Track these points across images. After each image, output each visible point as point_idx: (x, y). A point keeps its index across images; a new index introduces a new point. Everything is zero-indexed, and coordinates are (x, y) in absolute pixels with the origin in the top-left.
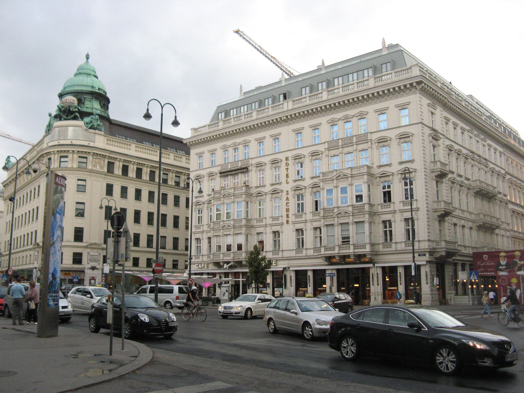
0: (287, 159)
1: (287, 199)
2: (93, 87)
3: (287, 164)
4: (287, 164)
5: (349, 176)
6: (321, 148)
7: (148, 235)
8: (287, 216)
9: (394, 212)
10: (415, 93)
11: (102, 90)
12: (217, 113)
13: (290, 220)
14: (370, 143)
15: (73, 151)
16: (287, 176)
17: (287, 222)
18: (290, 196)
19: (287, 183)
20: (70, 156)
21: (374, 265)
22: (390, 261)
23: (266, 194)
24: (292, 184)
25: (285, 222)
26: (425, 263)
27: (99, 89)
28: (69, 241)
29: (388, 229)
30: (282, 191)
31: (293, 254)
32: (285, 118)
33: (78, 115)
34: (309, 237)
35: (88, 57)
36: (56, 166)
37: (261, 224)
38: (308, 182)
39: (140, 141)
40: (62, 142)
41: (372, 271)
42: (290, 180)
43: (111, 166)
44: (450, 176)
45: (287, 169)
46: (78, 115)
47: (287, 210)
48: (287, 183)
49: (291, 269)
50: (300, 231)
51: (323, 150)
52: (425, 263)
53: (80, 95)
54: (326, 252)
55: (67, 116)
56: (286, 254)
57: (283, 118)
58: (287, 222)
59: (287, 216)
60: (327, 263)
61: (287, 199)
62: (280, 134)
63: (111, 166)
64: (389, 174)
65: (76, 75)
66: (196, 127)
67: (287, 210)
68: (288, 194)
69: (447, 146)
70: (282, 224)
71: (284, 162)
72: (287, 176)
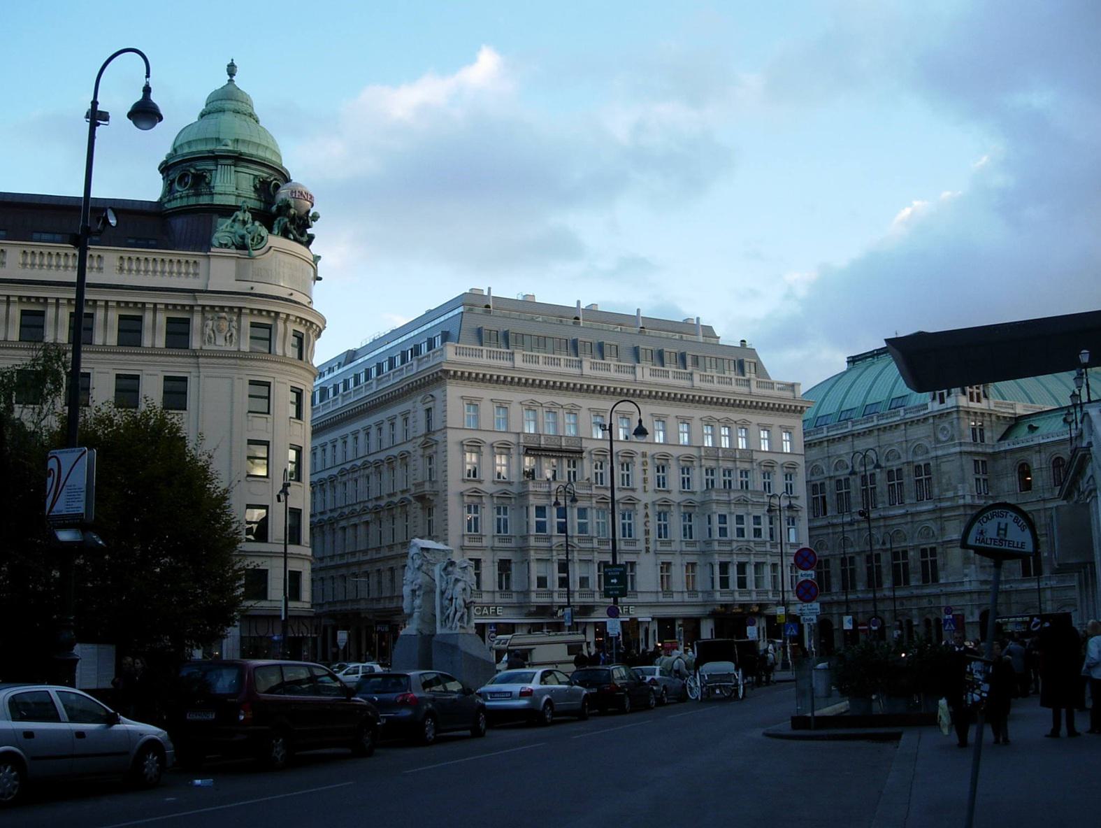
1: (647, 515)
8: (647, 541)
13: (651, 550)
17: (647, 550)
19: (645, 491)
32: (648, 393)
34: (678, 575)
35: (231, 70)
45: (645, 470)
47: (647, 532)
48: (645, 491)
50: (666, 566)
56: (641, 598)
57: (644, 392)
58: (647, 550)
59: (647, 541)
61: (647, 515)
67: (647, 532)
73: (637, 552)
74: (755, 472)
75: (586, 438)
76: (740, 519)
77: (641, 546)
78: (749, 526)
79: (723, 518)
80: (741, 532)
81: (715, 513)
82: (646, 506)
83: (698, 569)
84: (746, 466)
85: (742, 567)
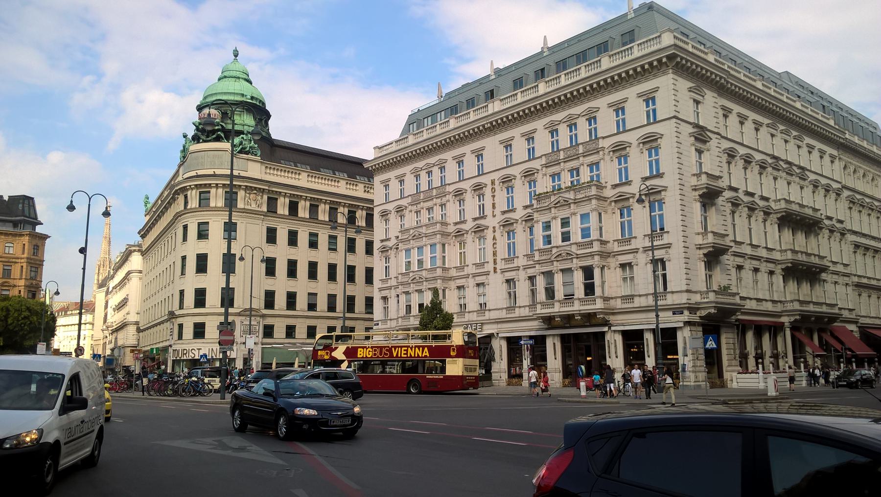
0: (493, 183)
1: (494, 238)
2: (243, 95)
3: (493, 190)
4: (493, 190)
5: (571, 201)
7: (309, 294)
8: (495, 262)
9: (635, 251)
10: (665, 73)
11: (257, 99)
12: (409, 123)
13: (498, 267)
14: (601, 153)
15: (217, 184)
17: (495, 271)
18: (498, 234)
20: (213, 191)
21: (610, 328)
22: (633, 322)
23: (467, 232)
24: (500, 217)
25: (492, 270)
26: (681, 325)
27: (252, 98)
28: (214, 307)
30: (487, 228)
31: (503, 314)
33: (222, 135)
36: (193, 206)
38: (519, 214)
39: (316, 168)
40: (200, 172)
41: (608, 337)
42: (497, 212)
43: (272, 203)
44: (728, 194)
45: (494, 196)
46: (222, 135)
47: (495, 254)
48: (494, 216)
49: (500, 335)
51: (539, 168)
52: (681, 325)
53: (227, 108)
54: (544, 311)
55: (208, 137)
58: (495, 271)
59: (495, 262)
60: (546, 326)
61: (494, 238)
62: (483, 149)
63: (272, 203)
64: (628, 196)
65: (219, 80)
66: (380, 145)
67: (495, 254)
68: (494, 232)
69: (725, 150)
71: (489, 187)
72: (494, 205)
73: (487, 274)
76: (565, 223)
77: (489, 267)
78: (576, 227)
80: (566, 237)
81: (537, 222)
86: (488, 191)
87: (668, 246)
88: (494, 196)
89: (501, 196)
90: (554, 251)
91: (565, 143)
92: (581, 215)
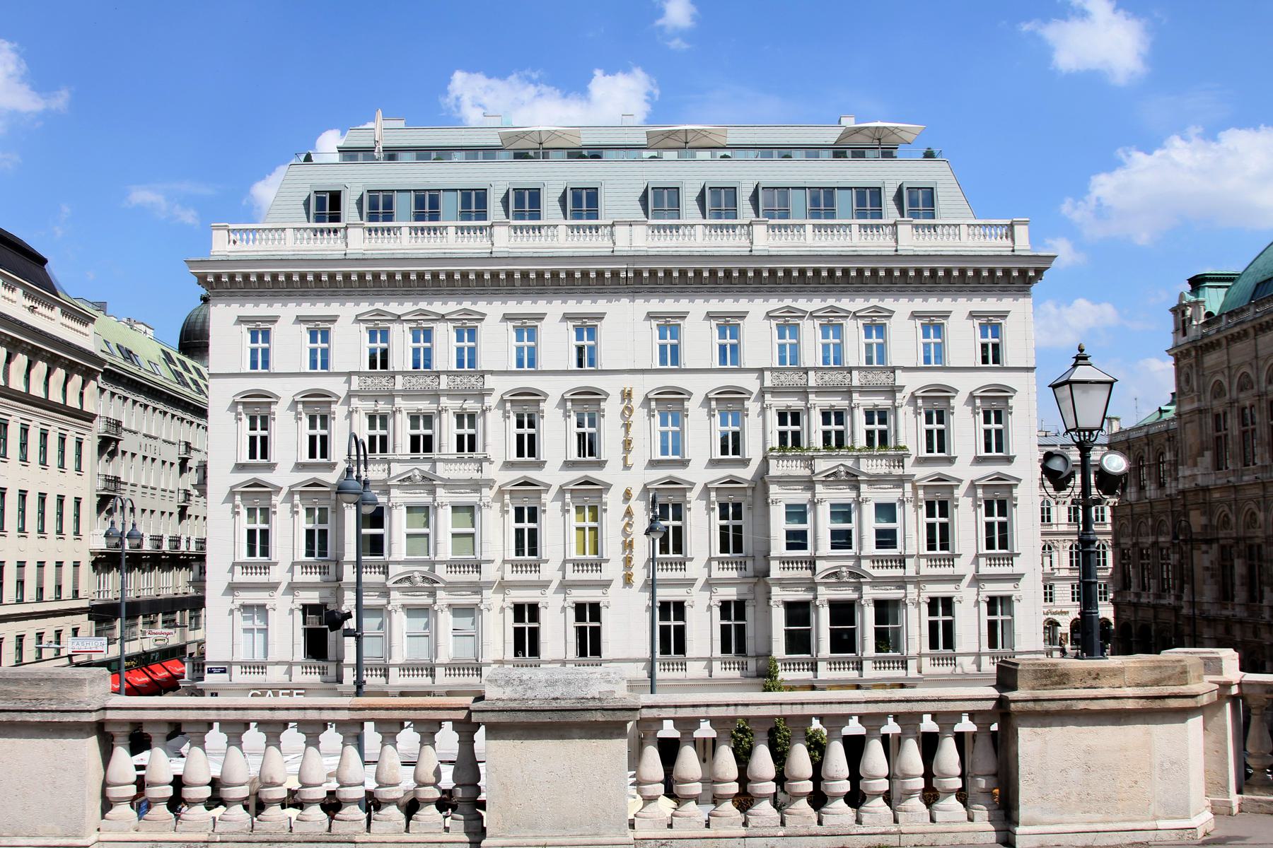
0: (627, 395)
1: (629, 513)
6: (750, 383)
8: (628, 562)
16: (627, 445)
17: (628, 580)
19: (626, 467)
29: (940, 618)
30: (608, 487)
32: (631, 275)
37: (533, 577)
42: (639, 456)
45: (627, 426)
48: (626, 467)
57: (623, 275)
58: (628, 580)
59: (628, 562)
61: (629, 513)
70: (605, 585)
72: (627, 445)
73: (605, 585)
74: (900, 411)
75: (492, 372)
76: (842, 513)
77: (612, 570)
79: (797, 513)
80: (841, 539)
81: (776, 502)
82: (627, 496)
83: (749, 611)
84: (881, 402)
85: (885, 610)
86: (612, 408)
87: (1016, 578)
88: (627, 426)
89: (648, 432)
90: (821, 566)
91: (811, 355)
92: (877, 505)
